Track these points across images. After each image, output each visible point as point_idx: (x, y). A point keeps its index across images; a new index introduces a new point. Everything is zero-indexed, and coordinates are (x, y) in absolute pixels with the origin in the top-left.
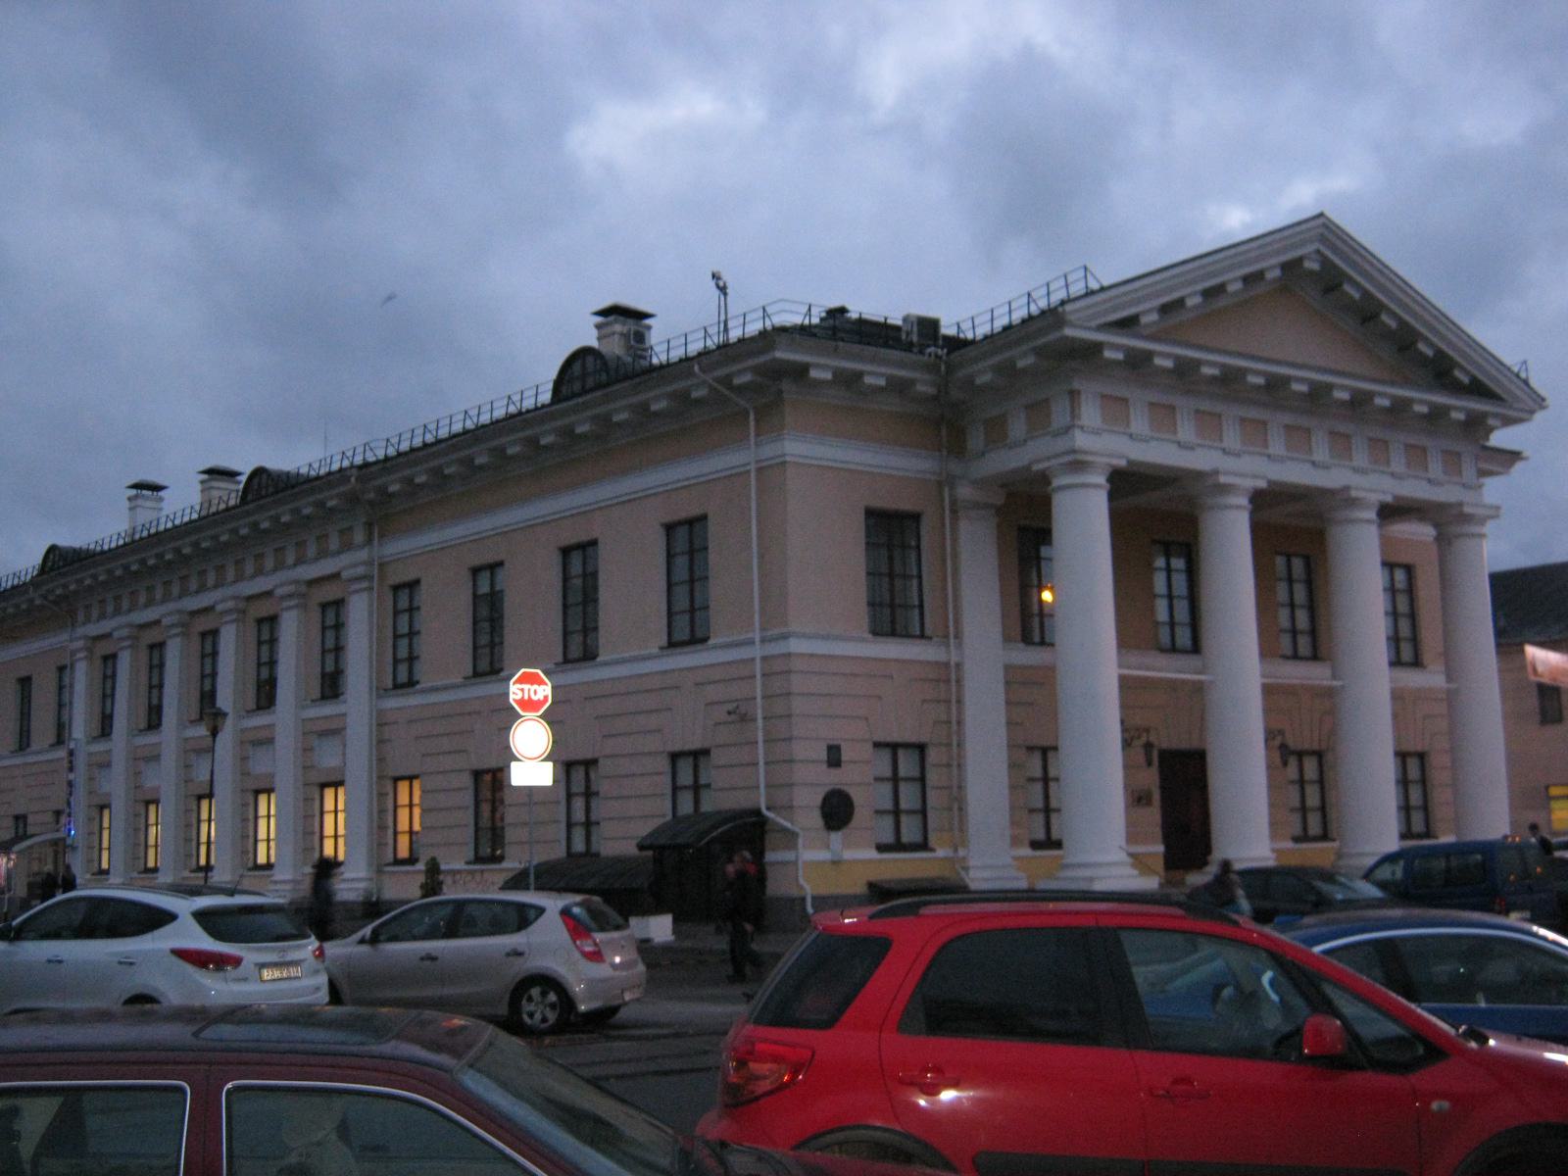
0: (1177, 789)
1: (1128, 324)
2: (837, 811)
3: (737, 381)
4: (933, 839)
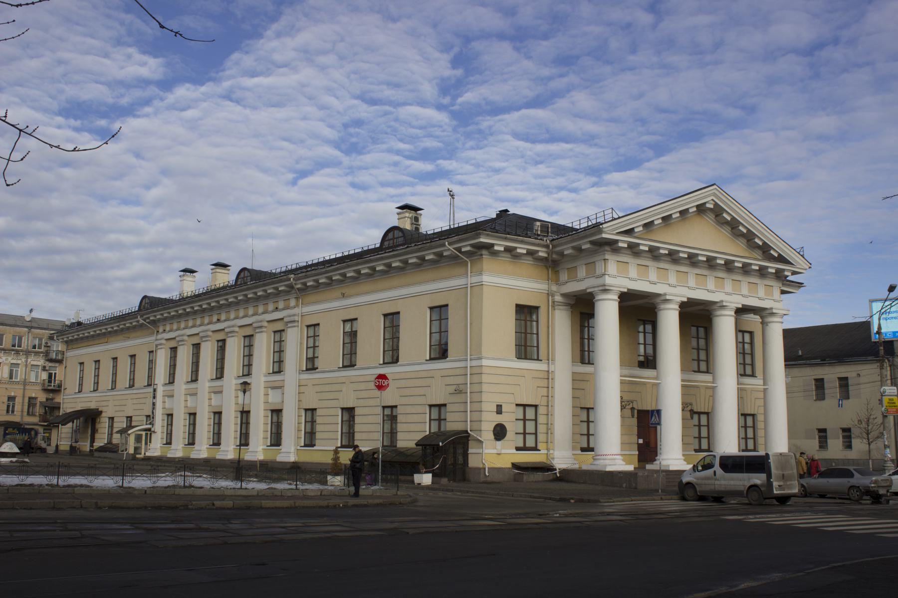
0: (645, 425)
1: (629, 232)
2: (500, 432)
3: (463, 250)
4: (540, 446)
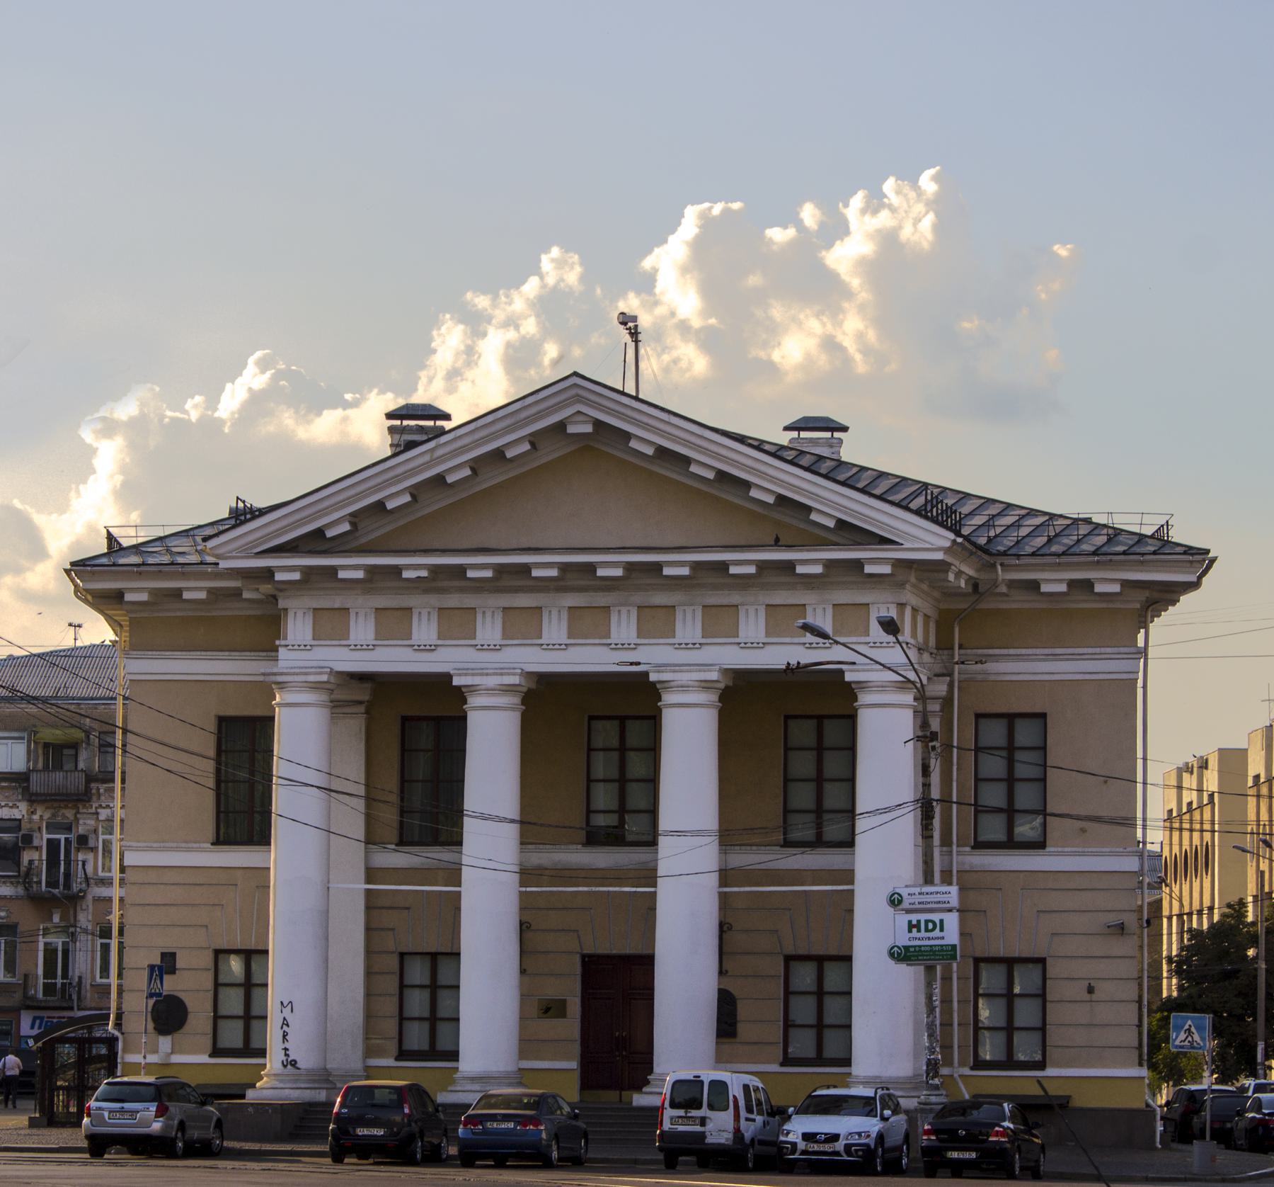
0: (607, 997)
1: (315, 541)
2: (169, 1016)
